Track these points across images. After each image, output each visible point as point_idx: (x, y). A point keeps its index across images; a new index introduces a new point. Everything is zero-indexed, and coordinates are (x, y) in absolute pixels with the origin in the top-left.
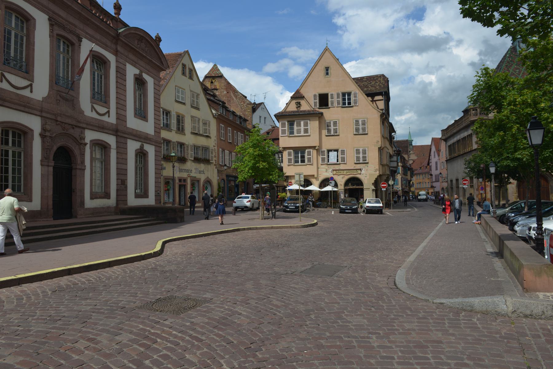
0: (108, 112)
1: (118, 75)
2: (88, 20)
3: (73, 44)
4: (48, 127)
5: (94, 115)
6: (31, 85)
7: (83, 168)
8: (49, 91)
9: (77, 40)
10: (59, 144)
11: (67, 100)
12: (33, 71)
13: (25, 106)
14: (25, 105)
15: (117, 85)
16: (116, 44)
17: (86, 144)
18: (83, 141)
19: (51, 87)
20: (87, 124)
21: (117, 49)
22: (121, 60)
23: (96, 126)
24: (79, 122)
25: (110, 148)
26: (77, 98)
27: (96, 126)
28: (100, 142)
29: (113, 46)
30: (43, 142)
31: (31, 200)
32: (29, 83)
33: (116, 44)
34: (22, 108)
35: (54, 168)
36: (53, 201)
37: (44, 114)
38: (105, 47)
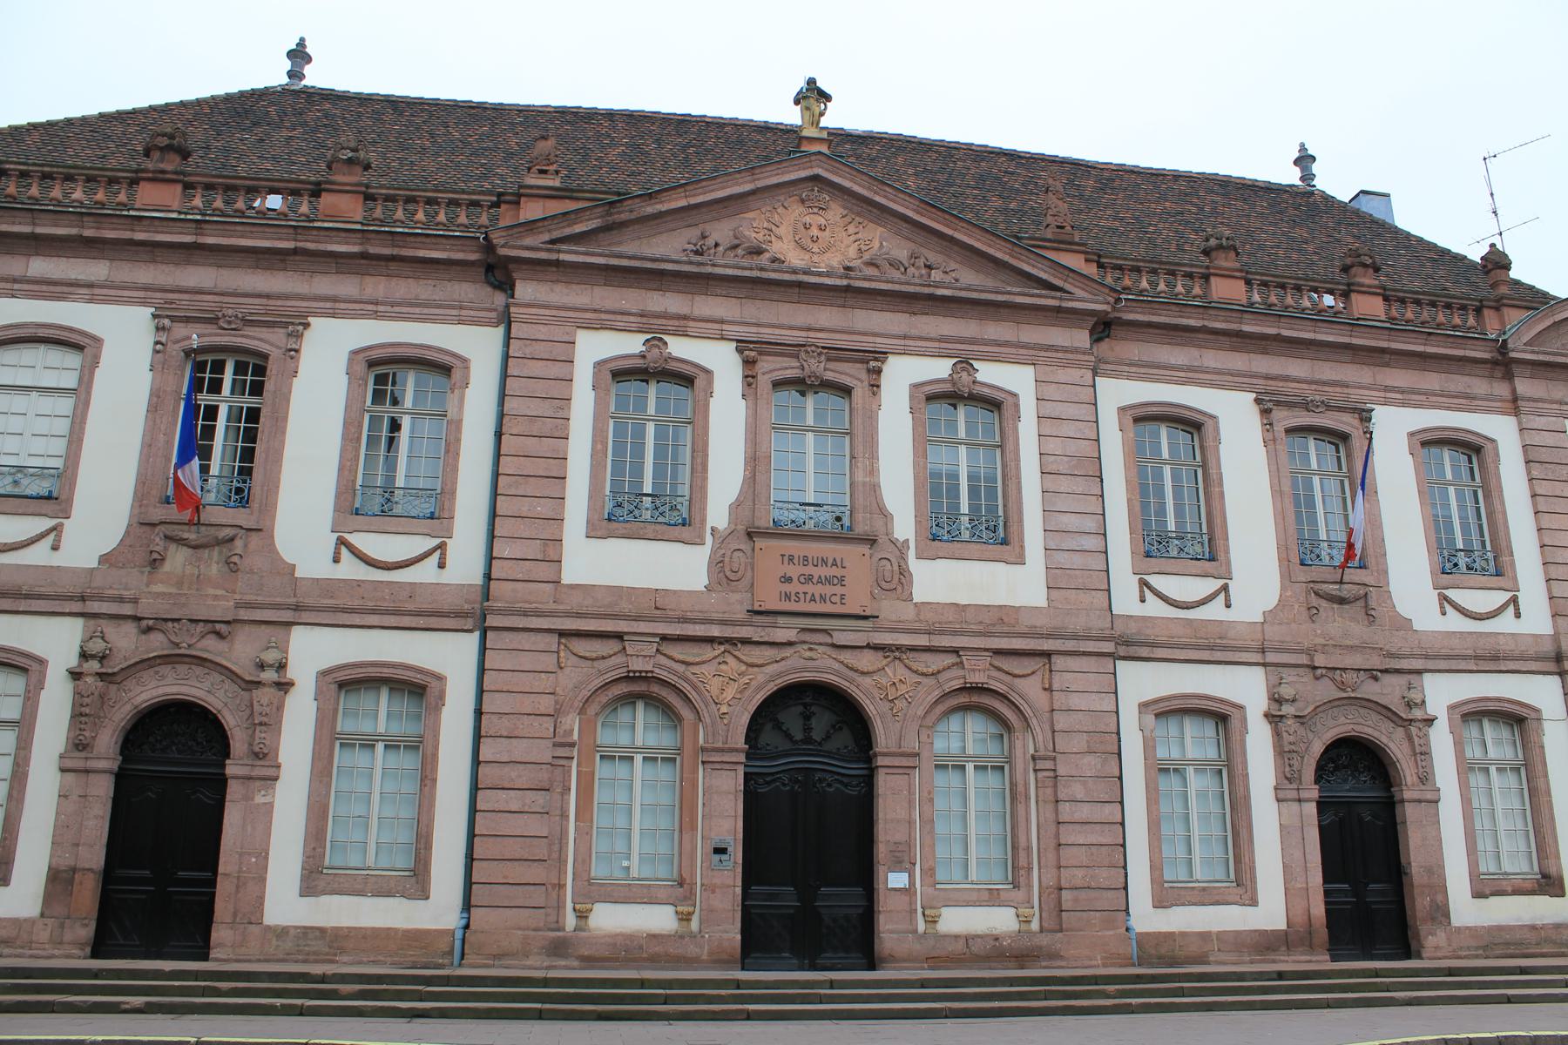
1: (1535, 473)
2: (1383, 351)
3: (1345, 437)
4: (1286, 691)
5: (1455, 623)
6: (1225, 588)
7: (1429, 796)
8: (1283, 588)
9: (1356, 422)
10: (1330, 735)
11: (1342, 601)
12: (1227, 552)
13: (1211, 648)
14: (1214, 647)
15: (1535, 504)
16: (1509, 377)
17: (1430, 721)
18: (1417, 713)
19: (1287, 576)
20: (1427, 657)
21: (1514, 391)
22: (1539, 422)
23: (1465, 657)
24: (1391, 656)
25: (1539, 719)
26: (1383, 587)
27: (1465, 657)
28: (1492, 706)
29: (1502, 389)
30: (1277, 734)
31: (1254, 902)
32: (1221, 582)
33: (1509, 377)
34: (1205, 655)
35: (1322, 806)
36: (1327, 903)
37: (1271, 657)
38: (1468, 402)
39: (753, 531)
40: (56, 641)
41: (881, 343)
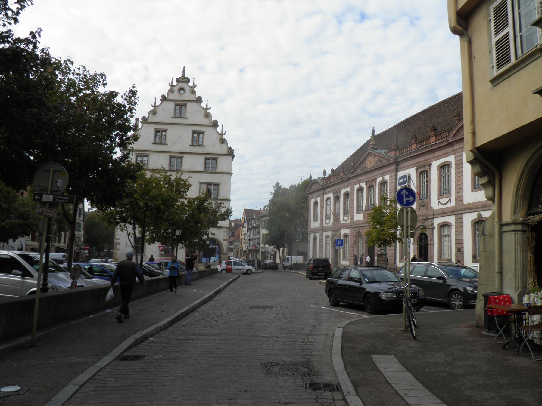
0: (450, 200)
5: (441, 207)
39: (366, 210)
40: (329, 233)
41: (376, 177)
